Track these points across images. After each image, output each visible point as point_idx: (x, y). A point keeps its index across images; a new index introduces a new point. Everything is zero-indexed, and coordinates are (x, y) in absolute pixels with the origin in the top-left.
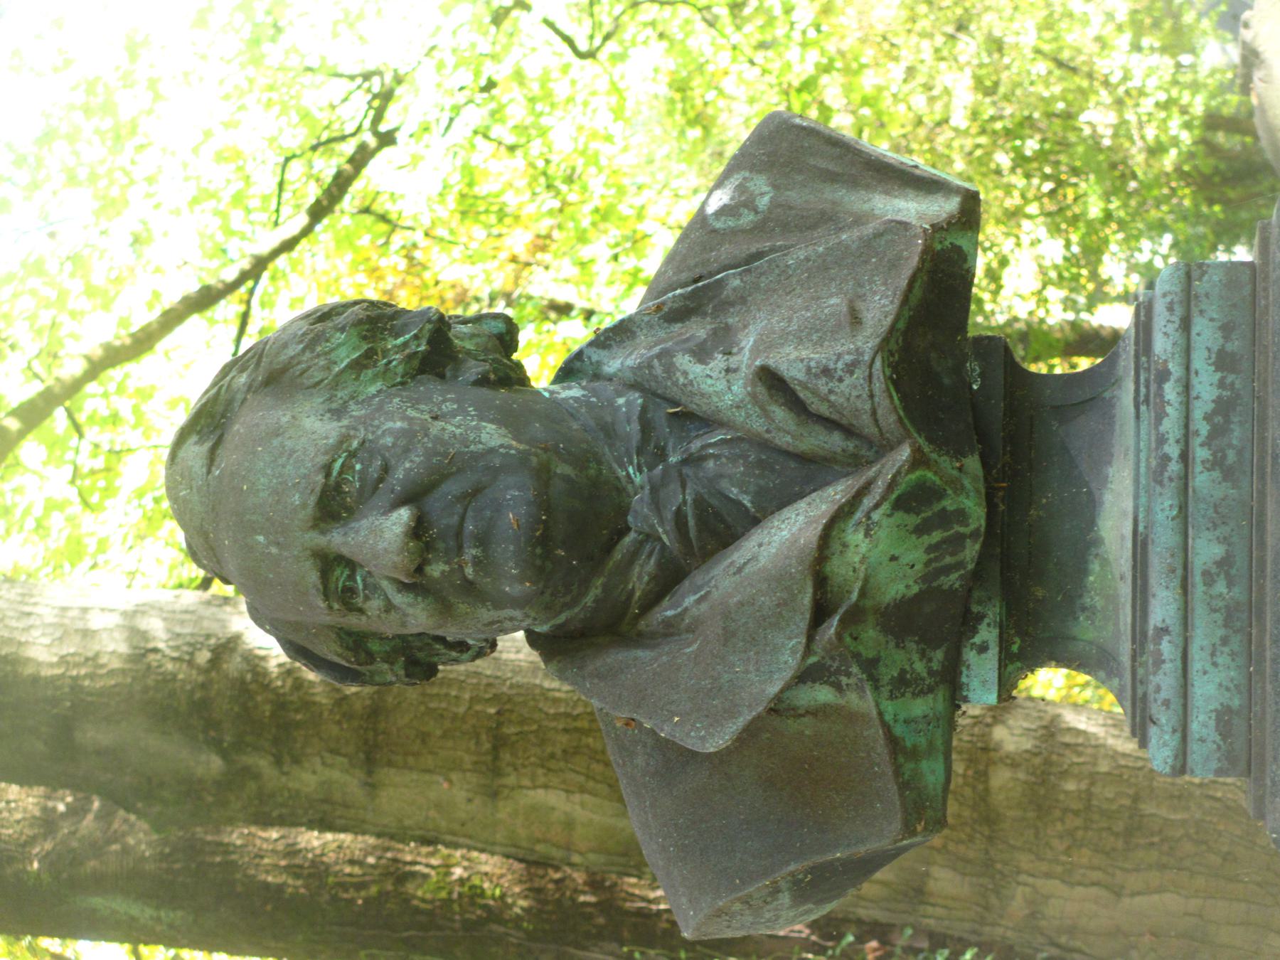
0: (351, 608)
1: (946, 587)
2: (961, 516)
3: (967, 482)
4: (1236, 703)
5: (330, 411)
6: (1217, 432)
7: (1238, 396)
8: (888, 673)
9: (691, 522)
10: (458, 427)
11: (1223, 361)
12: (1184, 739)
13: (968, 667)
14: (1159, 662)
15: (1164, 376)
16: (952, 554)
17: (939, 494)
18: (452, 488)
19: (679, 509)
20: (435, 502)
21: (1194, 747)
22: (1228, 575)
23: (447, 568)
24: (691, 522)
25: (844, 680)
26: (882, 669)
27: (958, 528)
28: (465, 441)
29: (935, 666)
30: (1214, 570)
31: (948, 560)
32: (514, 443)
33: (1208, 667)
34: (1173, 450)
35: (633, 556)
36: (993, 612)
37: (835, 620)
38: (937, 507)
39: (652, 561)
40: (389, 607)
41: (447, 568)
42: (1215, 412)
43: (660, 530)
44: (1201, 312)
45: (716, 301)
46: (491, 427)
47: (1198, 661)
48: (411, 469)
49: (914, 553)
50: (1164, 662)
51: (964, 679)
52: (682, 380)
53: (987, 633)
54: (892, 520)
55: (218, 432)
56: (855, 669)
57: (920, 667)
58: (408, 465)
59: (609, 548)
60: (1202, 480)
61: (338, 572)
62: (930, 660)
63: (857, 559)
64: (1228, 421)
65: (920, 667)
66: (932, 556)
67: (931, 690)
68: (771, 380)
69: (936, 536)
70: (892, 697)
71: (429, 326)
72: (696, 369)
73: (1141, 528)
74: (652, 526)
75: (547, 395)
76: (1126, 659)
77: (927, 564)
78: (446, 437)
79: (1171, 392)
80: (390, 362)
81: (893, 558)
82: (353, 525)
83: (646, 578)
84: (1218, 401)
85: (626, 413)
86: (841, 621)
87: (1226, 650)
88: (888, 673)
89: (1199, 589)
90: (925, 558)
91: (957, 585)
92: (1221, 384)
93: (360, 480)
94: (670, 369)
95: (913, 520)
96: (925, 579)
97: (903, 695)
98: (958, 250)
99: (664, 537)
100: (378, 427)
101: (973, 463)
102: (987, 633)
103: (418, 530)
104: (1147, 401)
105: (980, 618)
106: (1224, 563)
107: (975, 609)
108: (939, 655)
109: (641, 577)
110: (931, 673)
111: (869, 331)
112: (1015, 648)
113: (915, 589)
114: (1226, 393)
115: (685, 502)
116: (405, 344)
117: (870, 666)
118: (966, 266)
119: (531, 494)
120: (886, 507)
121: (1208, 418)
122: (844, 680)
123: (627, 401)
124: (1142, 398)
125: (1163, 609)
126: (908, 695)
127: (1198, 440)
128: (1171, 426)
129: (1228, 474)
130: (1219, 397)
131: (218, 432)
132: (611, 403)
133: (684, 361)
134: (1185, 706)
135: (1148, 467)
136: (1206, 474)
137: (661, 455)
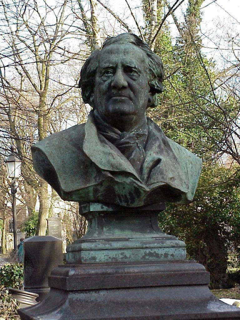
1: (116, 199)
4: (97, 260)
6: (151, 254)
7: (159, 258)
8: (99, 187)
9: (127, 145)
11: (166, 255)
13: (98, 205)
14: (105, 244)
22: (123, 258)
24: (127, 145)
31: (123, 199)
33: (104, 255)
36: (110, 209)
37: (111, 176)
39: (116, 137)
44: (176, 250)
50: (105, 245)
51: (95, 204)
53: (105, 208)
55: (136, 44)
56: (100, 180)
57: (100, 194)
59: (116, 127)
60: (142, 251)
61: (112, 70)
64: (154, 256)
66: (124, 196)
68: (159, 161)
69: (129, 197)
70: (93, 188)
71: (160, 89)
76: (102, 237)
77: (122, 195)
81: (124, 188)
86: (111, 177)
87: (108, 258)
88: (99, 187)
89: (120, 252)
90: (123, 195)
91: (116, 202)
92: (162, 255)
93: (133, 75)
102: (105, 208)
104: (156, 240)
105: (108, 206)
106: (126, 257)
108: (101, 198)
116: (156, 84)
117: (101, 184)
120: (136, 186)
121: (155, 252)
124: (157, 238)
127: (150, 250)
129: (144, 257)
130: (159, 254)
131: (136, 44)
134: (96, 250)
135: (144, 240)
136: (144, 252)
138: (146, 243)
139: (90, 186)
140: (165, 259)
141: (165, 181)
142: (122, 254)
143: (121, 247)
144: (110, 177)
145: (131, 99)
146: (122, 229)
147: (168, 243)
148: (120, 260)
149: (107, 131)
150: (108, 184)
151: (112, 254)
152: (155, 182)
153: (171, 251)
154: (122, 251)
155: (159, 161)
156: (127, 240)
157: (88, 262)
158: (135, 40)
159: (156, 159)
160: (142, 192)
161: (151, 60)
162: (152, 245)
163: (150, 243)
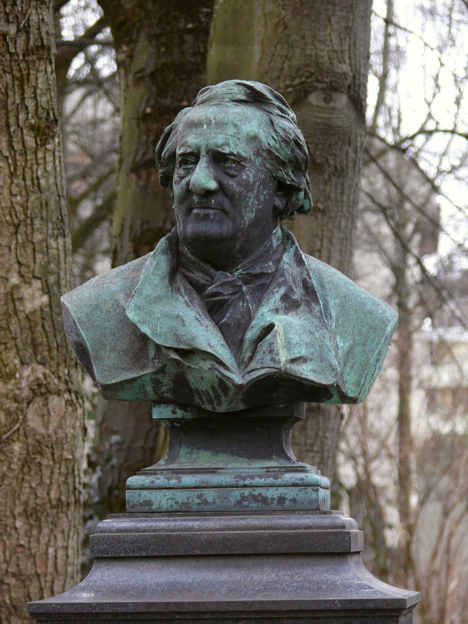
0: (181, 163)
2: (220, 404)
3: (233, 405)
4: (154, 507)
5: (258, 150)
6: (255, 498)
7: (268, 505)
8: (160, 377)
9: (216, 299)
10: (252, 203)
11: (281, 500)
12: (140, 489)
13: (167, 407)
14: (168, 479)
15: (276, 478)
16: (206, 400)
17: (226, 395)
18: (227, 204)
19: (222, 293)
20: (220, 198)
21: (138, 492)
22: (201, 503)
23: (196, 202)
24: (216, 299)
25: (156, 361)
26: (161, 375)
27: (215, 402)
28: (246, 207)
29: (165, 395)
30: (203, 498)
31: (204, 398)
32: (246, 226)
33: (167, 497)
34: (247, 482)
35: (206, 274)
36: (189, 416)
37: (177, 357)
38: (221, 394)
39: (204, 282)
40: (182, 178)
41: (196, 202)
42: (262, 497)
43: (214, 286)
44: (300, 491)
45: (310, 300)
46: (253, 215)
47: (169, 493)
48: (233, 187)
49: (203, 386)
50: (168, 480)
51: (162, 405)
52: (275, 290)
53: (180, 414)
54: (215, 378)
55: (251, 100)
56: (160, 365)
57: (164, 389)
58: (235, 186)
60: (236, 494)
61: (193, 157)
62: (167, 393)
63: (201, 365)
64: (259, 502)
65: (164, 389)
67: (156, 393)
68: (270, 328)
69: (212, 394)
70: (151, 379)
71: (297, 185)
72: (278, 296)
73: (219, 471)
74: (216, 282)
75: (274, 232)
76: (171, 466)
77: (202, 391)
78: (247, 199)
79: (270, 480)
80: (281, 171)
82: (211, 165)
83: (197, 279)
84: (266, 498)
85: (265, 267)
86: (177, 360)
87: (174, 503)
88: (160, 377)
90: (204, 390)
92: (273, 499)
93: (229, 167)
94: (280, 285)
95: (216, 385)
96: (197, 390)
97: (153, 383)
98: (331, 396)
99: (211, 288)
100: (251, 172)
101: (241, 407)
102: (180, 414)
103: (208, 193)
104: (268, 471)
105: (186, 411)
106: (206, 502)
107: (189, 409)
108: (170, 396)
109: (197, 276)
110: (163, 393)
111: (288, 366)
112: (175, 424)
113: (193, 386)
114: (269, 501)
115: (224, 295)
116: (289, 176)
118: (325, 400)
119: (225, 234)
120: (219, 375)
121: (260, 494)
122: (156, 361)
123: (270, 266)
124: (269, 470)
125: (188, 480)
126: (153, 385)
127: (252, 491)
128: (257, 481)
129: (239, 503)
130: (268, 498)
131: (251, 100)
132: (270, 260)
133: (282, 291)
135: (242, 473)
136: (239, 494)
137: (246, 283)
138: (244, 479)
139: (144, 375)
141: (277, 366)
142: (200, 496)
143: (198, 484)
144: (174, 359)
145: (224, 212)
147: (288, 477)
149: (191, 269)
150: (175, 371)
151: (181, 496)
152: (259, 367)
155: (270, 328)
156: (213, 471)
157: (138, 509)
158: (247, 94)
159: (267, 324)
160: (230, 385)
161: (273, 134)
163: (252, 477)
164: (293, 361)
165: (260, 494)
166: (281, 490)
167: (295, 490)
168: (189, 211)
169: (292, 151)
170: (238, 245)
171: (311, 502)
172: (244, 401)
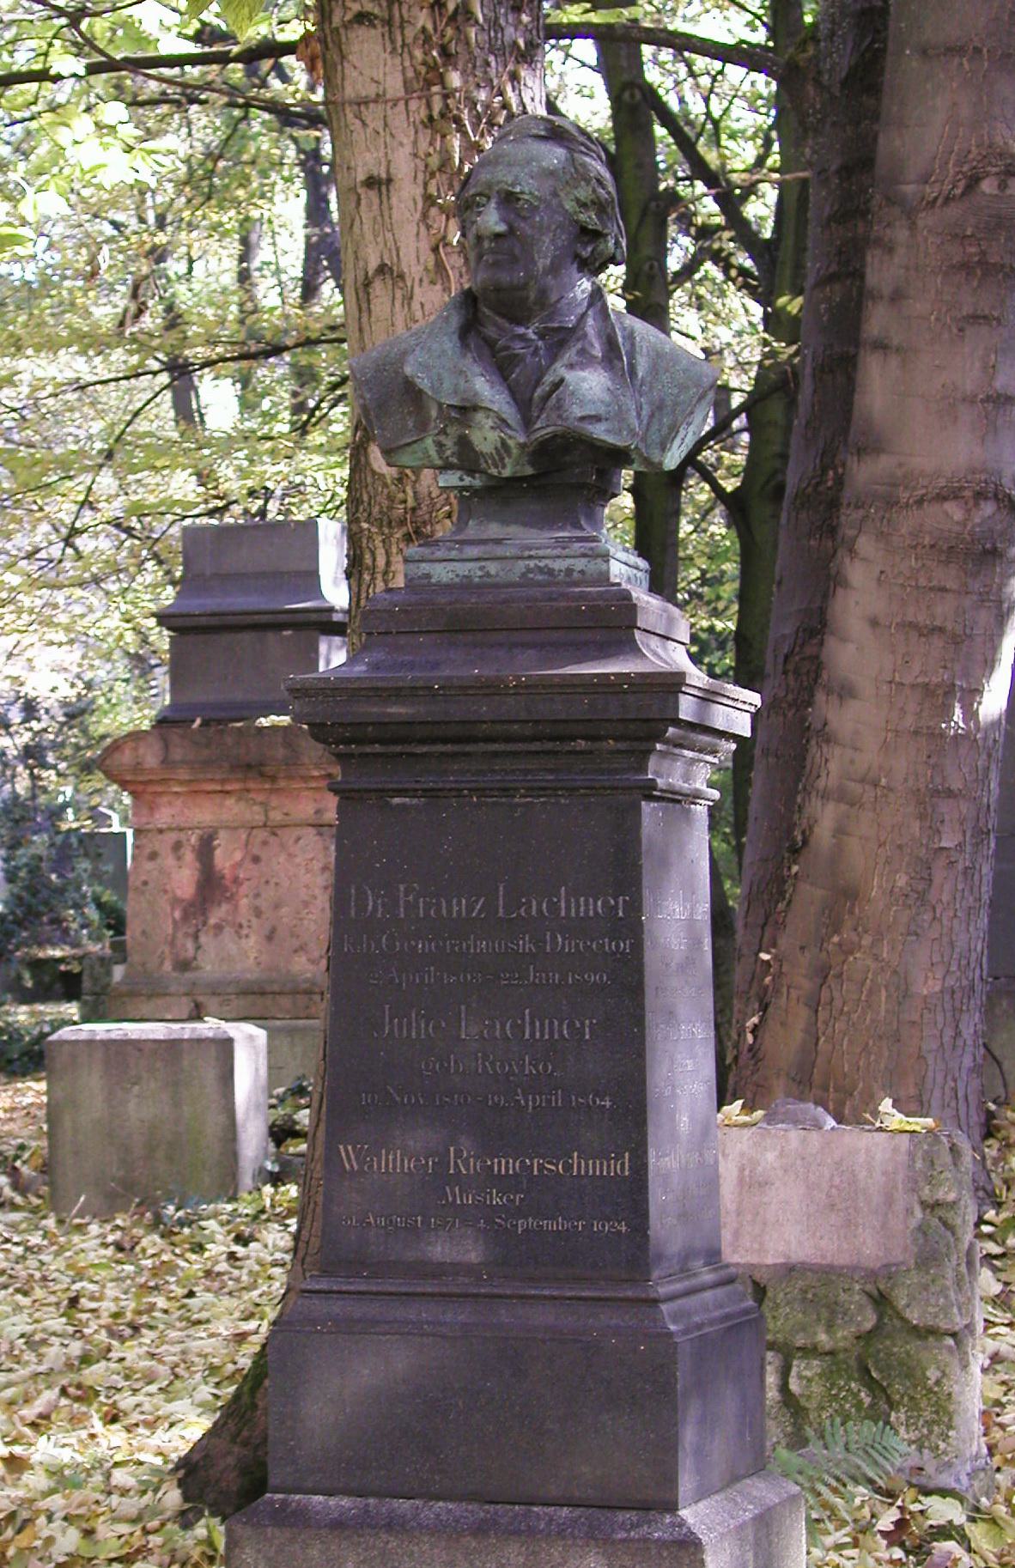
2: (504, 466)
4: (433, 580)
6: (540, 570)
8: (442, 438)
11: (569, 571)
36: (477, 482)
46: (548, 261)
53: (468, 481)
57: (448, 453)
60: (521, 564)
65: (448, 453)
76: (458, 538)
95: (499, 445)
101: (529, 471)
102: (468, 481)
103: (498, 236)
106: (488, 575)
129: (523, 575)
140: (568, 579)
142: (482, 568)
146: (505, 522)
148: (477, 580)
153: (580, 564)
154: (483, 564)
158: (546, 129)
162: (541, 553)
164: (582, 419)
165: (546, 566)
166: (569, 561)
167: (584, 561)
168: (480, 257)
169: (594, 191)
170: (532, 296)
171: (601, 573)
172: (532, 463)
